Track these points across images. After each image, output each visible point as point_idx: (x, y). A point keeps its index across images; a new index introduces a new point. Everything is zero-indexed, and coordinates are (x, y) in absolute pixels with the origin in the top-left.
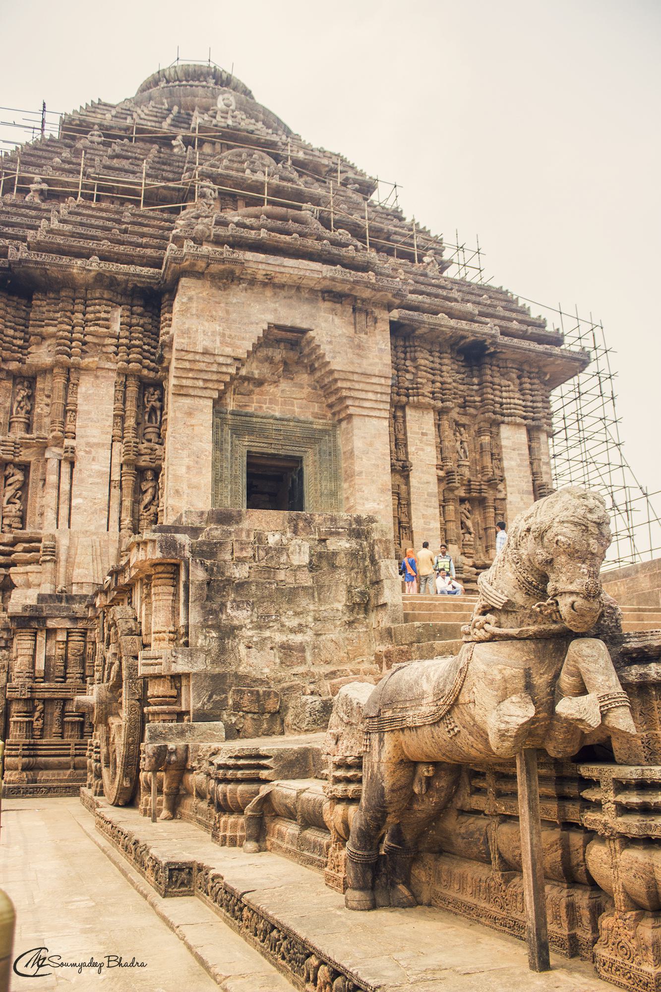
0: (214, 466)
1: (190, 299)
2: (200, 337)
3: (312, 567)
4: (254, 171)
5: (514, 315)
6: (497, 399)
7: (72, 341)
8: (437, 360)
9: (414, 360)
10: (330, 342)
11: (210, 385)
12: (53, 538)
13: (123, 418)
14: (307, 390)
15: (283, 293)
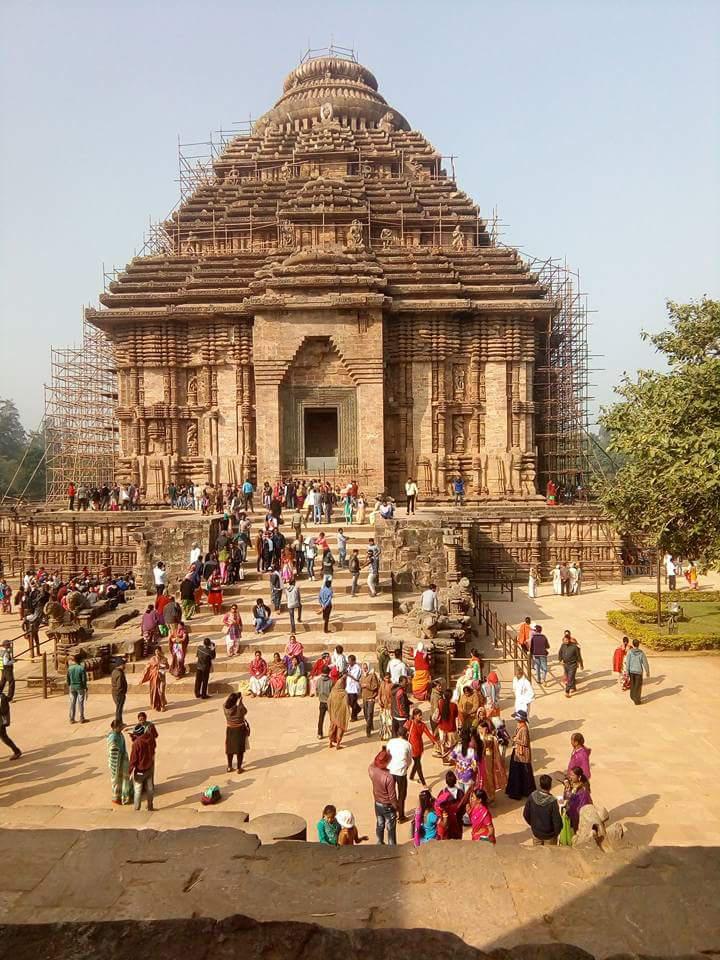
0: (284, 419)
1: (260, 329)
2: (267, 351)
3: (184, 540)
4: (317, 205)
5: (506, 277)
6: (483, 346)
7: (210, 350)
8: (435, 327)
9: (418, 330)
10: (343, 342)
11: (275, 377)
12: (210, 461)
13: (242, 391)
14: (336, 369)
15: (313, 315)
